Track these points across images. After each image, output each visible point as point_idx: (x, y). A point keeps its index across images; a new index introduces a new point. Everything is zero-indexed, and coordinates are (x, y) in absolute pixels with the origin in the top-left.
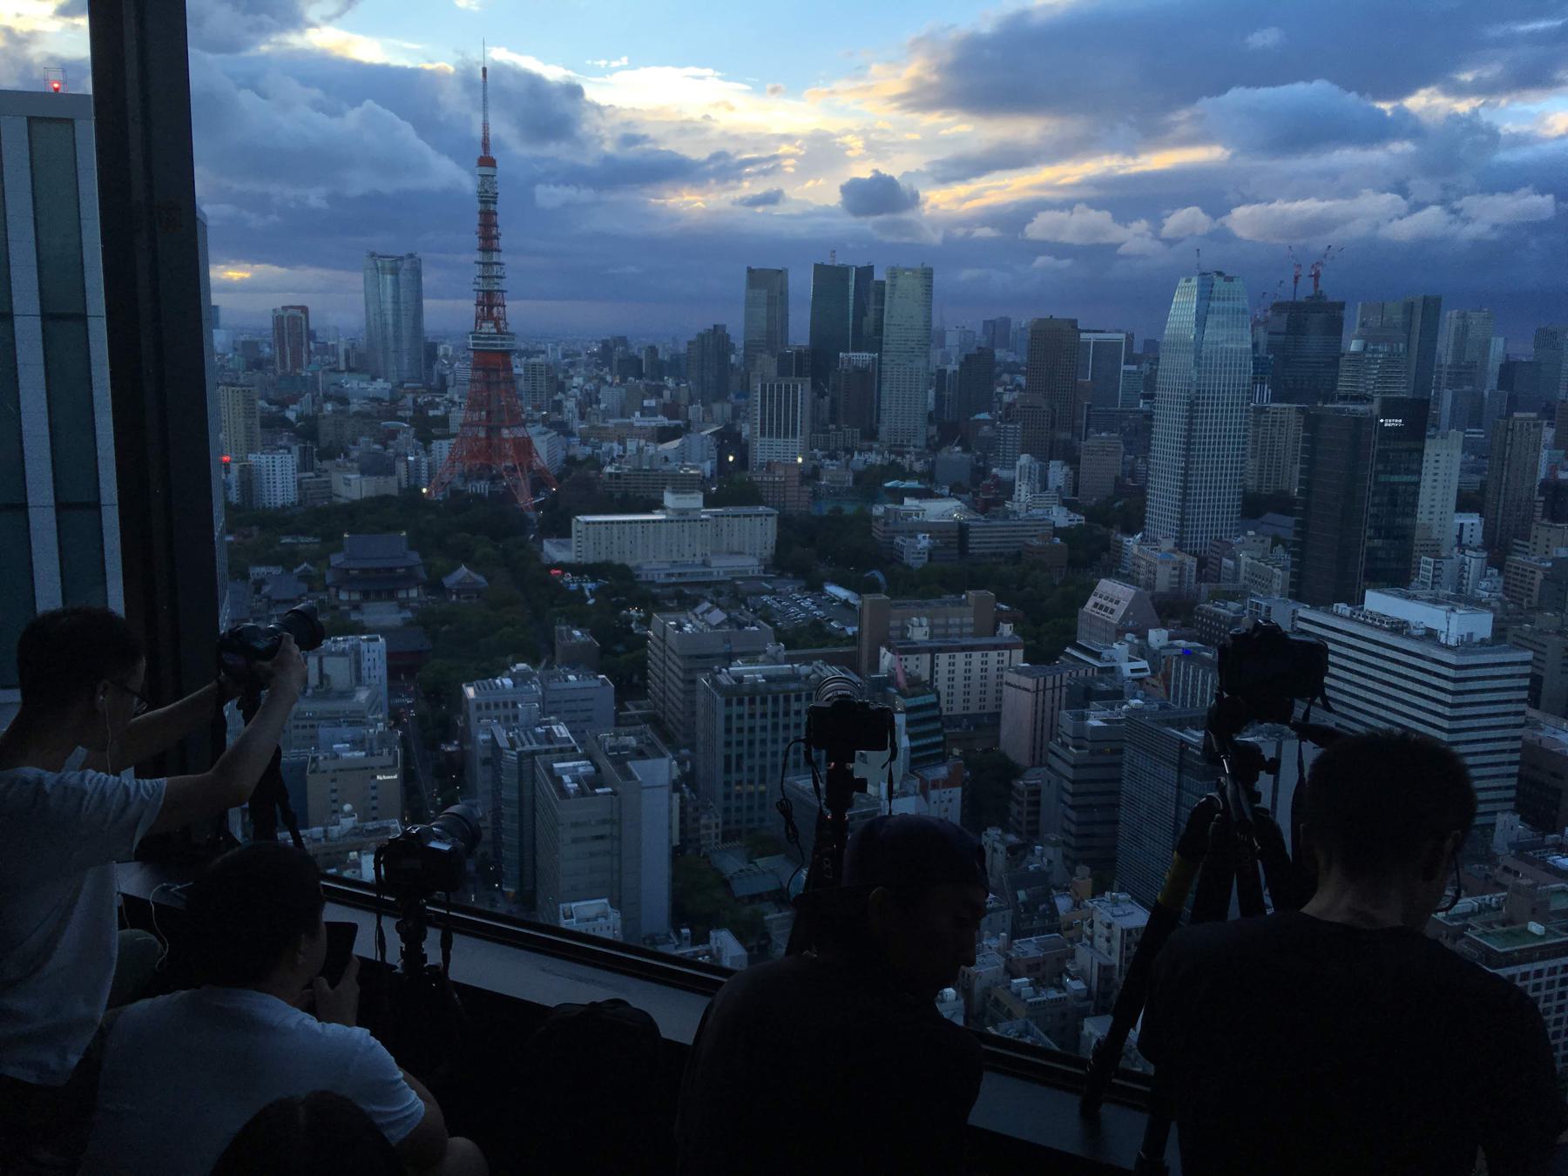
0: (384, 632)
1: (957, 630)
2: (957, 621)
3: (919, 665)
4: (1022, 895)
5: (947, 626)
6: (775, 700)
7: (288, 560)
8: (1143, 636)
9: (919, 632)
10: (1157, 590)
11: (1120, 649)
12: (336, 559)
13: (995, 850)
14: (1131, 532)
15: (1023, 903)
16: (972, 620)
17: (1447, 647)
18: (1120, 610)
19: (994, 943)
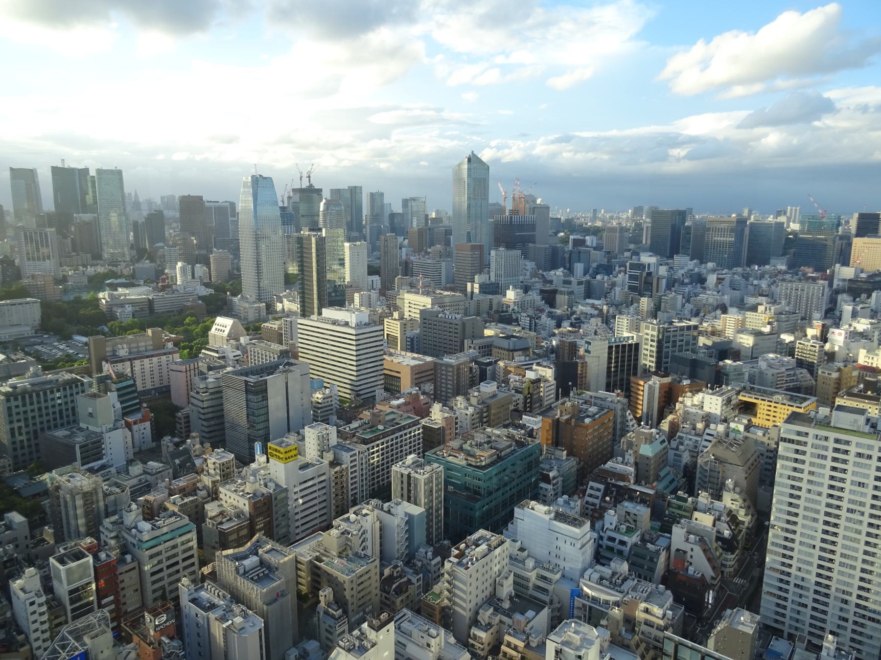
1: (144, 349)
2: (143, 344)
3: (126, 368)
4: (177, 461)
5: (138, 347)
6: (38, 395)
8: (237, 340)
9: (123, 352)
10: (249, 320)
13: (168, 447)
14: (234, 294)
15: (178, 465)
16: (151, 343)
17: (351, 327)
18: (227, 331)
19: (163, 484)
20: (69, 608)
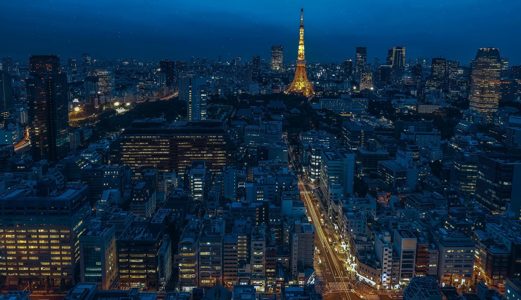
0: (281, 121)
2: (422, 128)
7: (258, 105)
8: (475, 135)
11: (469, 137)
12: (268, 106)
20: (402, 260)
